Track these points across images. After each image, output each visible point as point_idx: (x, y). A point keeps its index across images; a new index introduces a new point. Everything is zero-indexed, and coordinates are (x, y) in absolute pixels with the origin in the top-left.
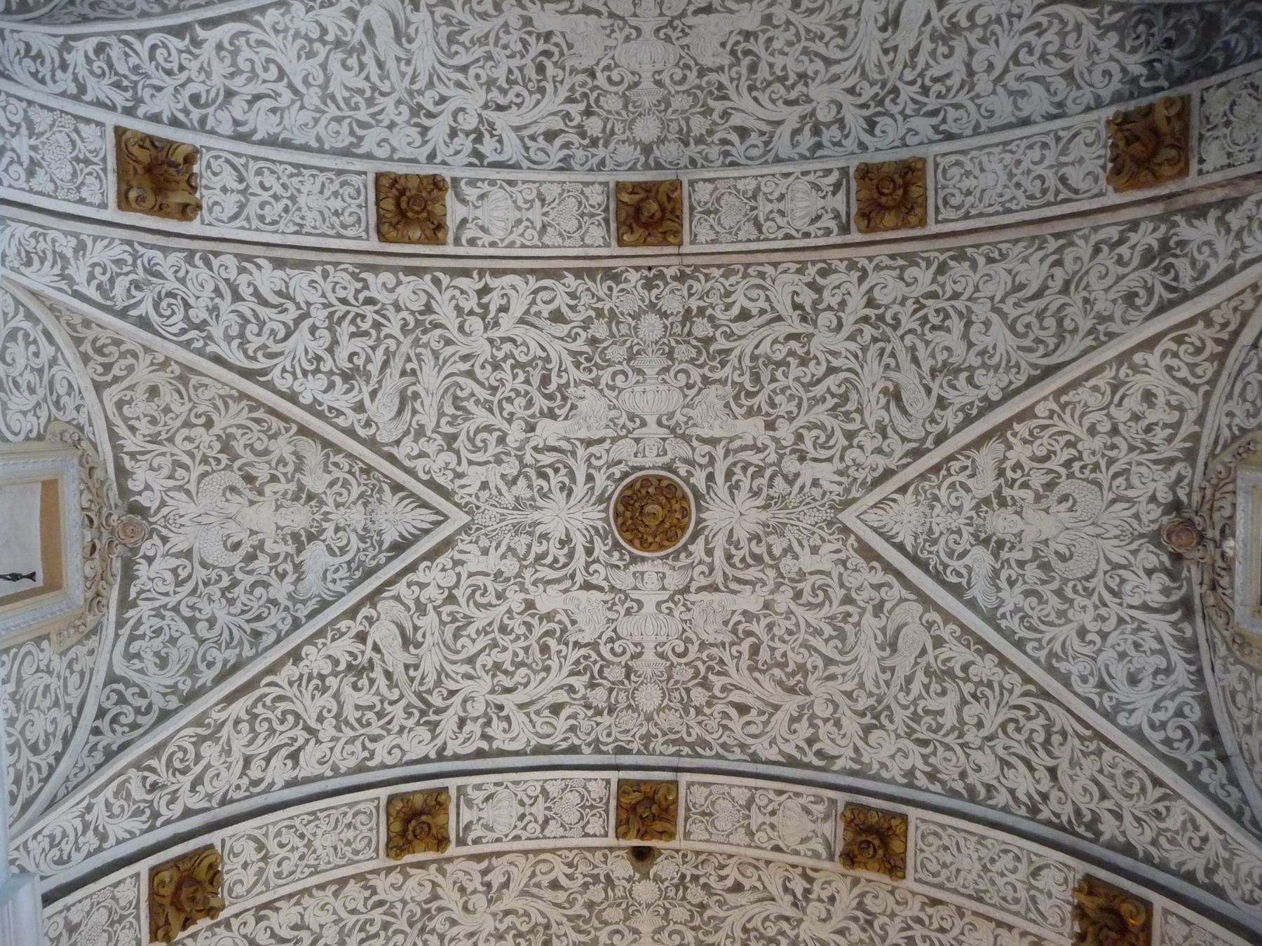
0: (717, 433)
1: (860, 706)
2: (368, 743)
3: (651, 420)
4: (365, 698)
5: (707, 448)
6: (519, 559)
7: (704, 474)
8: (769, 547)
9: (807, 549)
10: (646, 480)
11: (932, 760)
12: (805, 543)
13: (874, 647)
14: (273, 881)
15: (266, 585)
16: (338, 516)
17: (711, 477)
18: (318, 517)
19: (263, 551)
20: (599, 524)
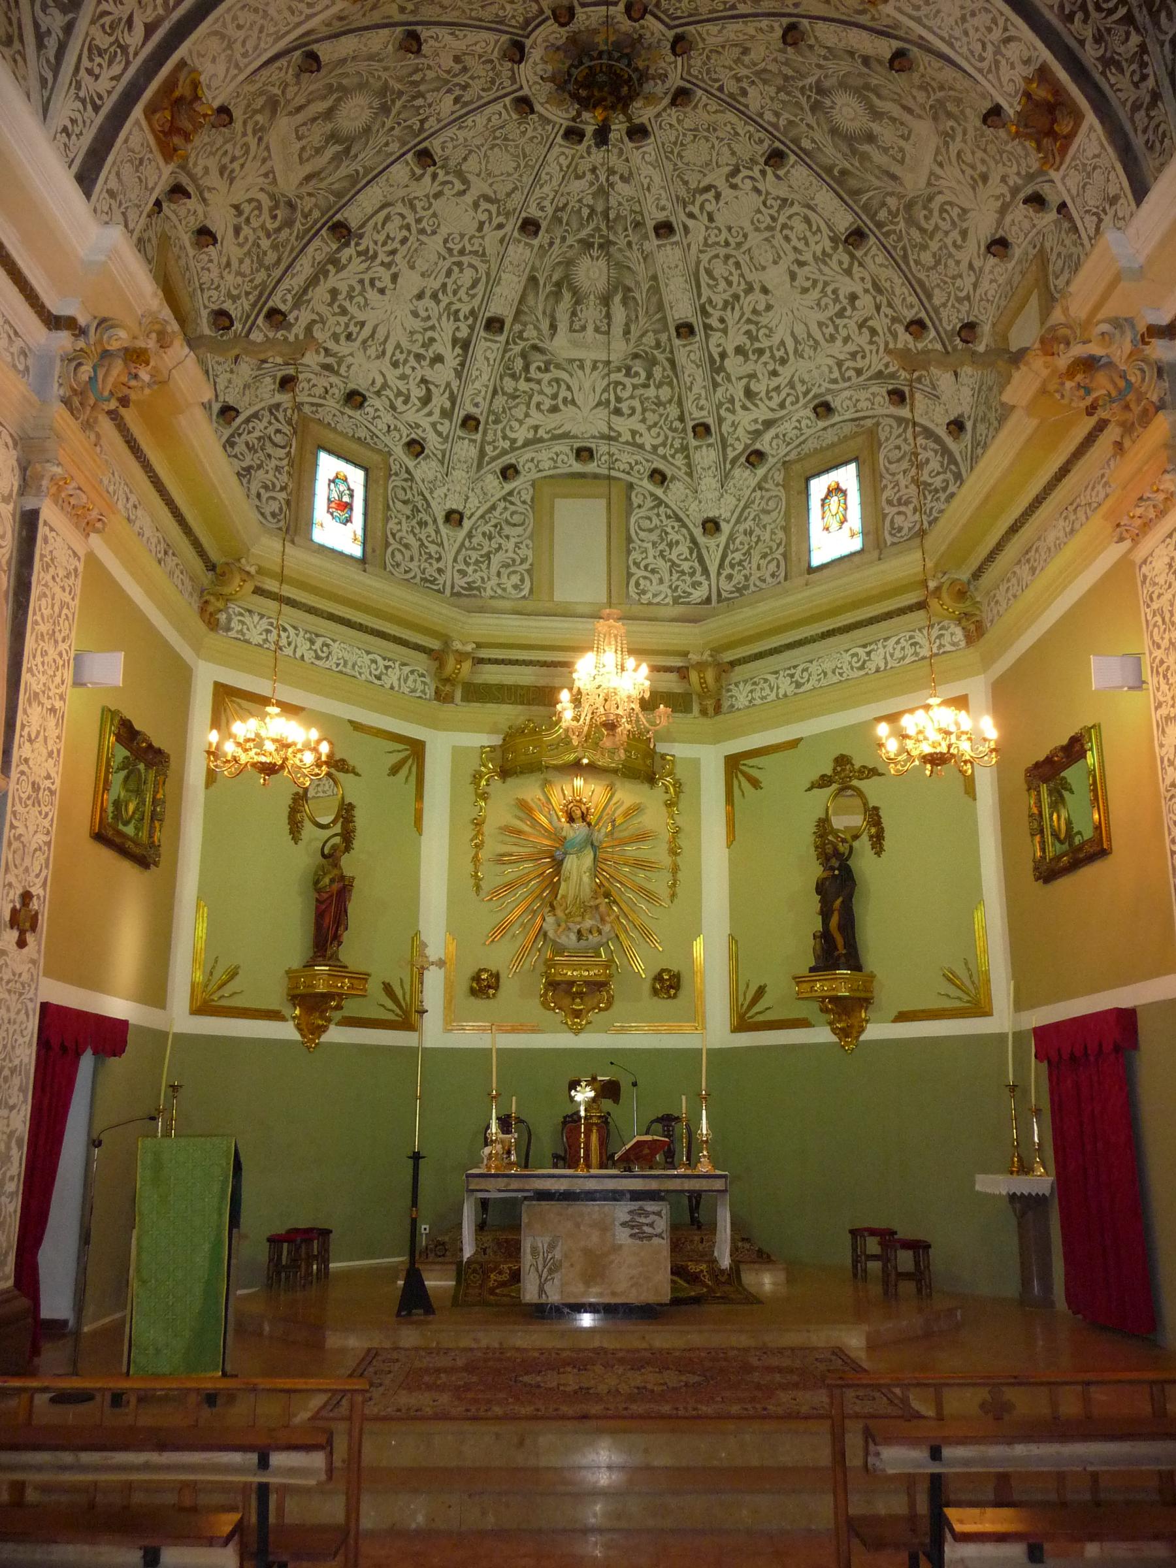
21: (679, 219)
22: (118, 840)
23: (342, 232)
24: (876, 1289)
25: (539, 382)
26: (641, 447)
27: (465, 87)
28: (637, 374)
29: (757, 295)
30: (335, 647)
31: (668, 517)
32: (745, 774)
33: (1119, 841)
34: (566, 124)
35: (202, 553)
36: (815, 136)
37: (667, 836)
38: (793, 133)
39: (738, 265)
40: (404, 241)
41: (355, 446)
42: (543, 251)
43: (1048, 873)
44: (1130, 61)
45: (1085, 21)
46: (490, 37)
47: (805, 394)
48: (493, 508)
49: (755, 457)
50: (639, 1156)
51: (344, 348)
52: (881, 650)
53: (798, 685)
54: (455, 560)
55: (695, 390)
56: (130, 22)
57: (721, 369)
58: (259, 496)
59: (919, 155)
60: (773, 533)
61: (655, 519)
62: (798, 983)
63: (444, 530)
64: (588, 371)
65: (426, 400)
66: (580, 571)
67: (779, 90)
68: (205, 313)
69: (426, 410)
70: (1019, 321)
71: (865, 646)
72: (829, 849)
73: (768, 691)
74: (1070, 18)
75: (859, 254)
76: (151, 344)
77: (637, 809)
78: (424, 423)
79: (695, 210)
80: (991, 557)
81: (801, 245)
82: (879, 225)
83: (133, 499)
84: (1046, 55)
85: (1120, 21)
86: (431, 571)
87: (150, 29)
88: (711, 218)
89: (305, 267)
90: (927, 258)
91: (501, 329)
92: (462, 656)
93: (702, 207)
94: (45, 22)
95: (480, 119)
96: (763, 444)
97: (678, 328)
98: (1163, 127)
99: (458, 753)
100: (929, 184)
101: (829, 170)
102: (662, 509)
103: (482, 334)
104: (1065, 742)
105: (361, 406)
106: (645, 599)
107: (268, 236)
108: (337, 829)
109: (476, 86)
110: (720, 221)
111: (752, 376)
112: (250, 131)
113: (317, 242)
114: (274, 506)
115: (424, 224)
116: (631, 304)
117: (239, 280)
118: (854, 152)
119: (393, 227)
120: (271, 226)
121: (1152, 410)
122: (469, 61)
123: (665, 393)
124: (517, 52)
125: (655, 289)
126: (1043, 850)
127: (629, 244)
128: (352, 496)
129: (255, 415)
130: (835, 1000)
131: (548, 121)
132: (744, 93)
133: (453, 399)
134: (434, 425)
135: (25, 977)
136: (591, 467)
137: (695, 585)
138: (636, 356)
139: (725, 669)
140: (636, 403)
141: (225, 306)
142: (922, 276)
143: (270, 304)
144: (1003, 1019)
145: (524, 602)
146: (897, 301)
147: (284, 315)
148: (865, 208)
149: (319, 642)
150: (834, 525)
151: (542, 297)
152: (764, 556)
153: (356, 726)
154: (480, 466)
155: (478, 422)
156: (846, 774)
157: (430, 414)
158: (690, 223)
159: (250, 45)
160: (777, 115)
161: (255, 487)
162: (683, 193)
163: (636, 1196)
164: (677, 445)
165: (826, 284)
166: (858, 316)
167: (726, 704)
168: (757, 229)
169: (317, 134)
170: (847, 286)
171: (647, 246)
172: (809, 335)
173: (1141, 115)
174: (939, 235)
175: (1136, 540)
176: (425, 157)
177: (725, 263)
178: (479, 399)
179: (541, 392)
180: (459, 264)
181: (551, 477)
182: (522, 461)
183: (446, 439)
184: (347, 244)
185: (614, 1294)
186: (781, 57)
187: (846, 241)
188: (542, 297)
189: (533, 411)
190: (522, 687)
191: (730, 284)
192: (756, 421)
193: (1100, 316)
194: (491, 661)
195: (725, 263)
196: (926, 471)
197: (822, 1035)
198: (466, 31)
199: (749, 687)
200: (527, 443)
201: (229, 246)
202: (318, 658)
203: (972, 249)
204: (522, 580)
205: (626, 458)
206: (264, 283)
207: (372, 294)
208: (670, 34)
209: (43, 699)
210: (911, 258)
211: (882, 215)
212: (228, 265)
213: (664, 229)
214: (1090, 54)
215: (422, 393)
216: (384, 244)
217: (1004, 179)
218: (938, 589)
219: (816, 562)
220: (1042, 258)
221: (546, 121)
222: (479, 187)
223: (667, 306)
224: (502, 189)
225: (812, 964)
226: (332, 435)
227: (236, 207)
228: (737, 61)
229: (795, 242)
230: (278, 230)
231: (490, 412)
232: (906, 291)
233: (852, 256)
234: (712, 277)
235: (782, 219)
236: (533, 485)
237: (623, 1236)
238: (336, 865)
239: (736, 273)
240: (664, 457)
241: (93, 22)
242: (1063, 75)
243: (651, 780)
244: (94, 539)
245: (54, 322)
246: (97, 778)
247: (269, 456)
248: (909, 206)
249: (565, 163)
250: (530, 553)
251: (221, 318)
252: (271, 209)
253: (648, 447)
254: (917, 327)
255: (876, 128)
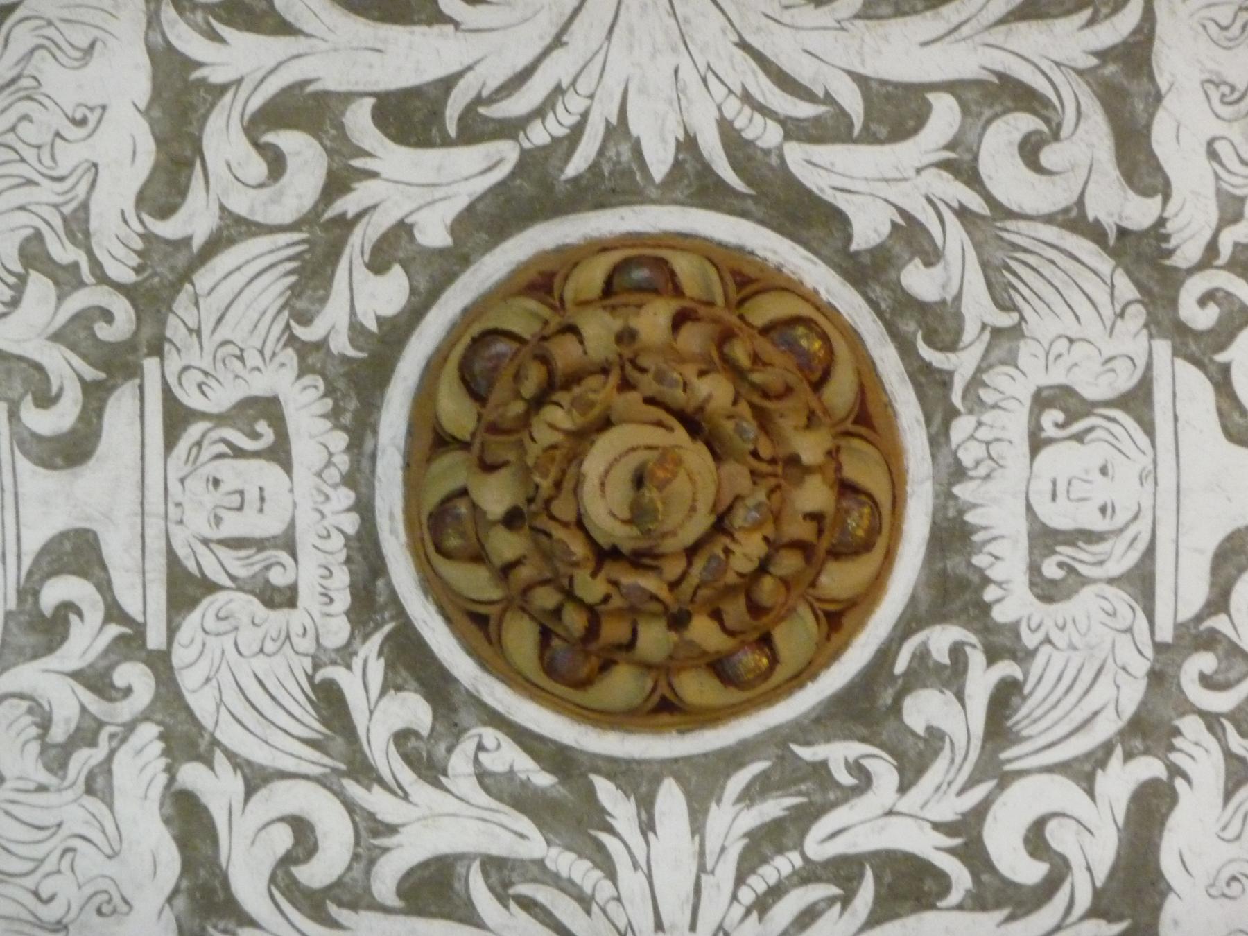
0: (125, 78)
3: (50, 505)
5: (224, 141)
7: (394, 160)
10: (442, 529)
17: (412, 116)
20: (731, 821)
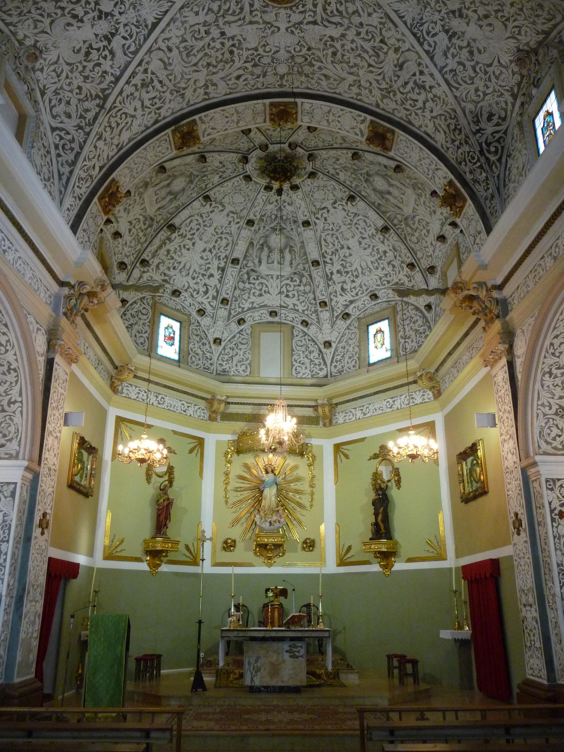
1: (382, 87)
2: (157, 111)
4: (152, 95)
6: (216, 14)
8: (346, 8)
9: (366, 13)
11: (409, 117)
12: (365, 10)
13: (392, 65)
14: (136, 175)
15: (99, 65)
16: (123, 19)
18: (113, 23)
19: (92, 49)
21: (312, 219)
22: (78, 487)
23: (172, 228)
24: (396, 681)
25: (254, 284)
26: (298, 311)
27: (224, 172)
28: (295, 281)
29: (345, 250)
30: (167, 399)
31: (309, 340)
32: (342, 453)
33: (492, 487)
34: (265, 184)
35: (112, 362)
36: (367, 191)
37: (309, 479)
38: (358, 189)
39: (337, 238)
40: (198, 229)
41: (175, 313)
42: (256, 232)
43: (467, 499)
44: (483, 182)
45: (466, 165)
46: (235, 155)
47: (366, 290)
48: (234, 336)
49: (346, 316)
50: (295, 620)
51: (172, 273)
52: (399, 400)
53: (365, 414)
54: (218, 359)
55: (320, 288)
56: (94, 167)
57: (331, 279)
58: (136, 336)
59: (409, 202)
60: (354, 348)
61: (304, 341)
62: (364, 545)
63: (213, 346)
64: (275, 279)
65: (206, 292)
66: (271, 367)
67: (352, 174)
68: (115, 264)
69: (206, 297)
70: (451, 268)
71: (392, 398)
72: (378, 487)
73: (351, 416)
74: (460, 163)
75: (387, 236)
76: (98, 289)
77: (296, 467)
78: (205, 302)
79: (319, 216)
80: (442, 364)
81: (363, 231)
82: (395, 225)
83: (87, 345)
84: (451, 176)
85: (477, 167)
86: (207, 364)
87: (101, 168)
88: (326, 219)
89: (157, 242)
90: (414, 239)
91: (238, 264)
92: (220, 401)
93: (322, 215)
94: (62, 170)
95: (230, 184)
96: (349, 310)
97: (313, 263)
98: (496, 208)
99: (218, 443)
100: (413, 212)
101: (373, 204)
102: (306, 337)
103: (230, 265)
104: (470, 445)
105: (179, 296)
106: (299, 376)
107: (142, 231)
108: (166, 478)
109: (228, 172)
110: (329, 220)
111: (344, 282)
112: (137, 194)
113: (162, 232)
114: (142, 340)
115: (206, 223)
116: (293, 253)
117: (130, 249)
118: (383, 197)
119: (193, 225)
120: (143, 228)
121: (495, 317)
122: (225, 163)
123: (307, 288)
124: (245, 160)
125: (303, 247)
126: (464, 489)
127: (292, 229)
128: (174, 334)
129: (135, 302)
130: (381, 553)
131: (258, 183)
132: (338, 174)
133: (217, 292)
134: (209, 303)
135: (43, 547)
136: (276, 319)
137: (321, 369)
138: (295, 273)
139: (333, 406)
140: (295, 293)
141: (124, 260)
142: (412, 246)
143: (142, 257)
144: (452, 562)
145: (247, 378)
146: (403, 255)
147: (148, 262)
148: (388, 218)
149: (160, 397)
150: (379, 346)
151: (255, 250)
152: (350, 358)
153: (175, 432)
154: (228, 320)
155: (228, 301)
156: (383, 454)
157: (208, 298)
158: (317, 221)
159: (139, 170)
160: (351, 182)
161: (134, 332)
162: (314, 210)
163: (292, 639)
164: (313, 309)
165: (374, 247)
166: (388, 260)
167: (334, 422)
168: (345, 224)
169: (163, 192)
170: (382, 248)
171: (299, 230)
172: (368, 266)
173: (488, 202)
174: (418, 231)
175: (492, 366)
176: (207, 198)
177: (332, 237)
178: (229, 292)
179: (255, 288)
180: (221, 238)
181: (259, 323)
182: (246, 317)
183: (214, 308)
184: (174, 232)
185: (282, 682)
186: (352, 162)
187: (381, 231)
188: (255, 250)
189: (251, 296)
190: (246, 414)
191: (334, 245)
192: (346, 301)
193: (474, 281)
194: (232, 403)
195: (332, 237)
196: (416, 325)
197: (376, 568)
198: (225, 153)
199: (344, 414)
200: (249, 309)
201: (127, 237)
202: (159, 404)
203: (431, 238)
204: (246, 368)
205: (291, 315)
206: (140, 250)
207: (184, 251)
208: (307, 153)
209: (53, 433)
210: (408, 239)
211: (396, 221)
212: (126, 244)
213: (306, 224)
214: (469, 177)
215: (204, 289)
216: (190, 231)
217: (442, 213)
218: (421, 376)
219: (372, 361)
220: (457, 245)
221: (256, 183)
222: (229, 208)
223: (308, 254)
224: (238, 209)
225: (371, 536)
226: (166, 309)
227: (130, 222)
228: (334, 163)
229: (360, 230)
230: (146, 229)
231: (233, 296)
232: (406, 251)
233: (384, 237)
234: (327, 243)
235: (355, 221)
236: (251, 327)
237: (286, 656)
238: (166, 494)
239: (336, 241)
240: (307, 315)
241: (80, 169)
242: (458, 185)
243: (302, 455)
244: (74, 365)
245: (62, 284)
246: (70, 462)
247: (140, 319)
248: (406, 219)
249: (265, 198)
250: (250, 356)
251: (122, 265)
252: (144, 222)
253: (300, 311)
254: (411, 266)
255: (391, 189)
